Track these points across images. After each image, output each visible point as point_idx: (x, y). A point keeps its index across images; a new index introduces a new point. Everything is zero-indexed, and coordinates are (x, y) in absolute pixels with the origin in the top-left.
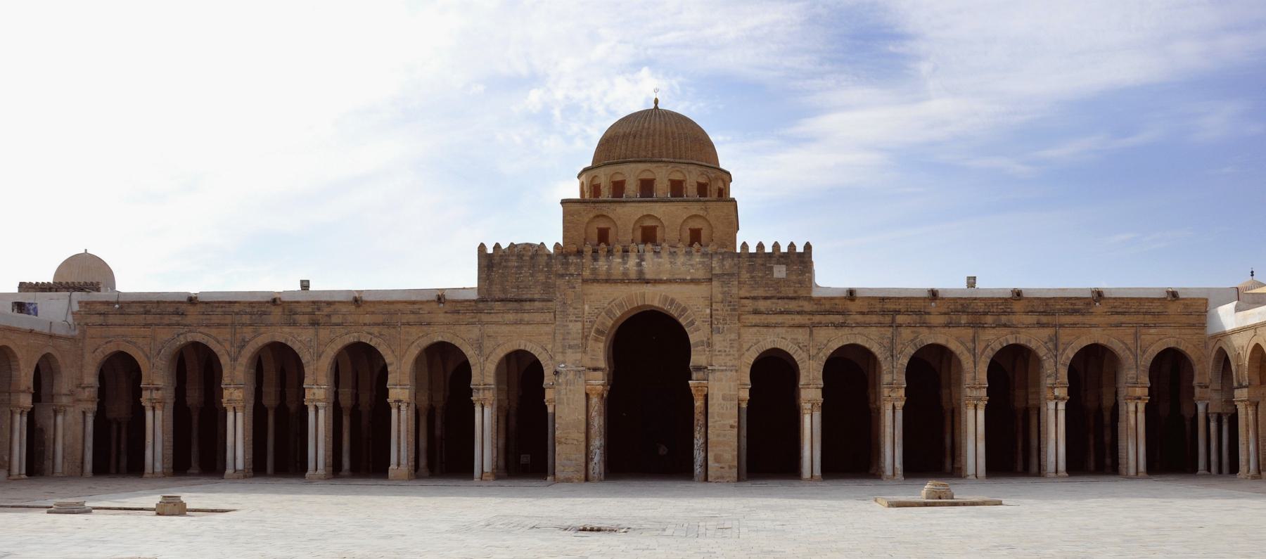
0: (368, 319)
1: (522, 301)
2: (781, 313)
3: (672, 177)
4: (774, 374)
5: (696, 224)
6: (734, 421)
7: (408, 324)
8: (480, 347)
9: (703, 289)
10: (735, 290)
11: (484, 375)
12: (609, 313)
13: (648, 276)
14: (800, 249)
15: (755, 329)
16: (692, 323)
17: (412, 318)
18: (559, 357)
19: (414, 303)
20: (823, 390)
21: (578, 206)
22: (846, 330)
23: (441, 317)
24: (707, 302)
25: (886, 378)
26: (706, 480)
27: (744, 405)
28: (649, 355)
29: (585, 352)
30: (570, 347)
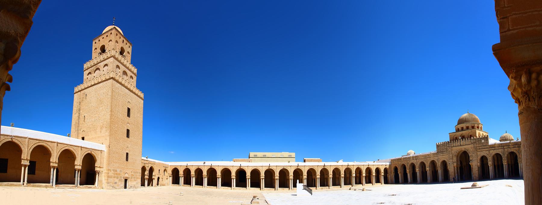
11: (439, 164)
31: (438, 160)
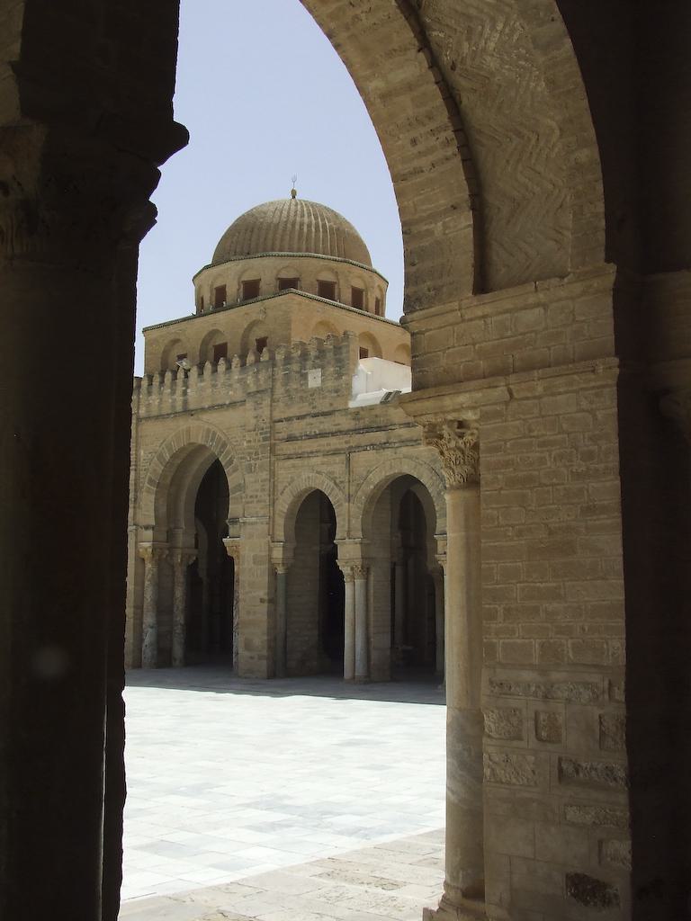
3: (245, 278)
5: (259, 333)
6: (263, 593)
12: (160, 457)
13: (191, 407)
15: (292, 461)
16: (231, 462)
21: (155, 334)
22: (388, 452)
27: (280, 570)
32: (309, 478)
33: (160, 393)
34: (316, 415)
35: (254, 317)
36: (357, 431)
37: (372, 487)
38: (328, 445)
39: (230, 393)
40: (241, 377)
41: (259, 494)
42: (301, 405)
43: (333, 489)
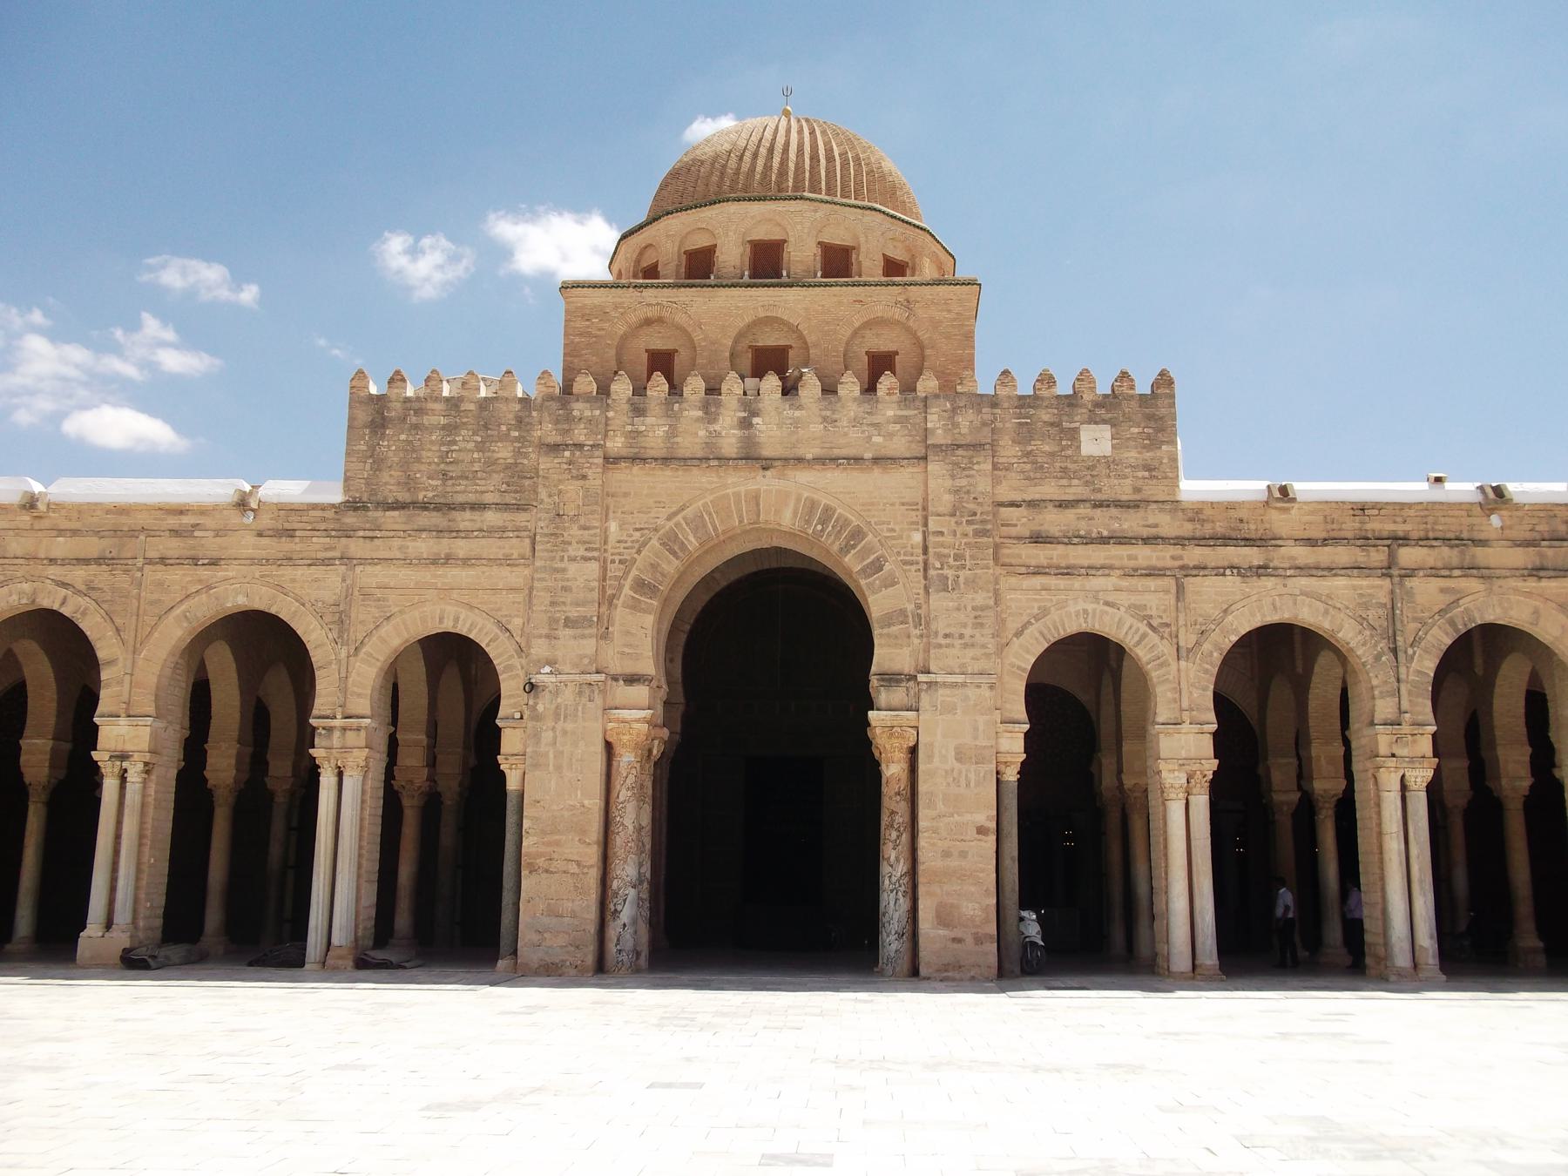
0: (62, 547)
1: (451, 507)
2: (1103, 540)
4: (1078, 702)
5: (883, 342)
6: (986, 817)
7: (163, 560)
8: (340, 620)
9: (900, 483)
10: (983, 485)
12: (671, 542)
13: (766, 452)
14: (1143, 387)
15: (1038, 581)
16: (877, 566)
17: (173, 547)
18: (539, 649)
19: (180, 511)
20: (1216, 736)
22: (1269, 583)
23: (247, 544)
24: (916, 516)
25: (1384, 708)
26: (914, 972)
27: (1012, 775)
28: (770, 679)
29: (605, 636)
30: (569, 623)
31: (340, 620)
32: (1085, 611)
33: (668, 412)
34: (1101, 506)
35: (879, 311)
36: (1200, 541)
37: (1234, 639)
38: (1130, 557)
39: (877, 439)
40: (900, 413)
41: (968, 632)
42: (1064, 482)
43: (1144, 636)
